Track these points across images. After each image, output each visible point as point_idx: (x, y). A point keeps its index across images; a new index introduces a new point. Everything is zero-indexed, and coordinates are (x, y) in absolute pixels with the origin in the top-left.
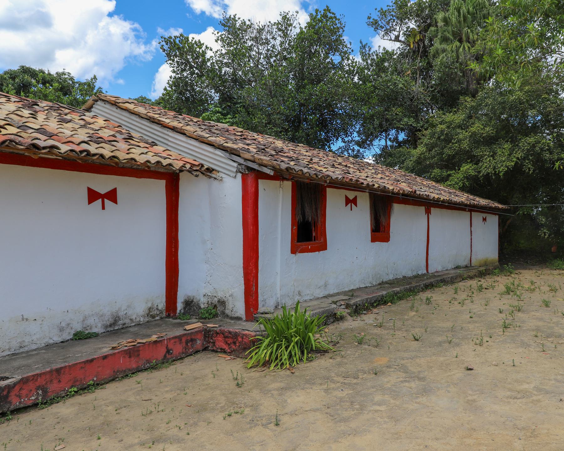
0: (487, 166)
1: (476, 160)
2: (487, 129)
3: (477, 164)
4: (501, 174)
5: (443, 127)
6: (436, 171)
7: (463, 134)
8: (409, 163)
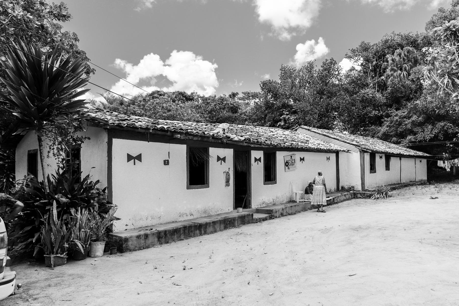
0: (420, 137)
1: (415, 134)
2: (420, 119)
3: (415, 135)
4: (428, 140)
5: (397, 118)
6: (394, 139)
8: (380, 135)
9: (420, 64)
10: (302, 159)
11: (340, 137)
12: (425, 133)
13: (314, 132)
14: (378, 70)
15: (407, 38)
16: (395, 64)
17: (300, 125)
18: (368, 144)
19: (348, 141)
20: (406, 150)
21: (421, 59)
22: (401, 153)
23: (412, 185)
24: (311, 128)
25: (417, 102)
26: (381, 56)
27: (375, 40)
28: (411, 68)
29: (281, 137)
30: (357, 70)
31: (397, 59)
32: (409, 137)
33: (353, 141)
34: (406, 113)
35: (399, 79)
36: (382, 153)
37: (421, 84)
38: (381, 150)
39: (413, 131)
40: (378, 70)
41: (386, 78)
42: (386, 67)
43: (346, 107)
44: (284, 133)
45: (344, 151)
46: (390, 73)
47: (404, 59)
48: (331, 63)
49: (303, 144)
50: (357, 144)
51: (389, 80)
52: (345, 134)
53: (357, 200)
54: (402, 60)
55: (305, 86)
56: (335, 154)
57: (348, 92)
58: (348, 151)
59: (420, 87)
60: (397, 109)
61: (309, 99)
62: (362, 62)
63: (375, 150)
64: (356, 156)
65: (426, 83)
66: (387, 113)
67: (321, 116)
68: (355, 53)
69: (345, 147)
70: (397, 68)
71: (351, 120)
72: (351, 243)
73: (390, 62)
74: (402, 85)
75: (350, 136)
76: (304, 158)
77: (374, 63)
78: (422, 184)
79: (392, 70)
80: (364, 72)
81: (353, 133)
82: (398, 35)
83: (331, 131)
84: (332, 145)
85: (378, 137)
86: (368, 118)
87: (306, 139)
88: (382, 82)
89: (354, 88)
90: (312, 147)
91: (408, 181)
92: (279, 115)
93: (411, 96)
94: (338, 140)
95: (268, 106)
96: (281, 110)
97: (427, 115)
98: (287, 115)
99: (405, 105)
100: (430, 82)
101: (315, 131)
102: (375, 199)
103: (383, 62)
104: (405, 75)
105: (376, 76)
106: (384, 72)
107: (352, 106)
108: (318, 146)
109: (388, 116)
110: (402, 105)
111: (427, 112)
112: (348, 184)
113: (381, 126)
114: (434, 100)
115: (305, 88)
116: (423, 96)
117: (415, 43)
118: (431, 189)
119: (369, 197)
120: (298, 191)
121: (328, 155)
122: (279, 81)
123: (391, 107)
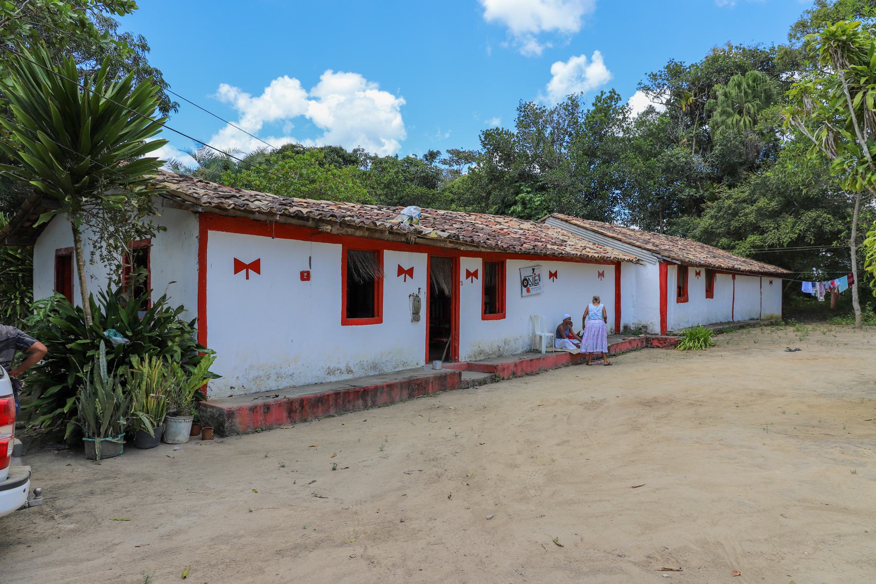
0: (771, 238)
1: (762, 232)
4: (785, 245)
5: (730, 202)
6: (724, 241)
7: (749, 209)
8: (697, 232)
9: (776, 103)
10: (553, 275)
11: (624, 234)
12: (782, 231)
13: (575, 225)
14: (697, 113)
15: (753, 54)
16: (730, 101)
17: (551, 212)
18: (675, 249)
19: (638, 244)
20: (744, 262)
21: (779, 94)
22: (736, 266)
23: (754, 326)
24: (570, 218)
25: (768, 174)
26: (704, 87)
27: (693, 56)
28: (758, 111)
29: (516, 233)
30: (658, 113)
31: (734, 92)
32: (751, 238)
33: (647, 242)
34: (747, 194)
35: (736, 130)
36: (700, 265)
37: (777, 140)
38: (698, 260)
39: (759, 227)
40: (698, 113)
41: (713, 127)
42: (713, 107)
43: (636, 181)
44: (522, 226)
45: (629, 261)
46: (719, 120)
47: (746, 93)
48: (611, 98)
49: (555, 247)
50: (654, 248)
51: (718, 132)
52: (633, 230)
53: (652, 350)
54: (743, 94)
55: (563, 140)
56: (613, 267)
57: (640, 153)
58: (638, 262)
59: (775, 147)
60: (730, 187)
61: (569, 164)
62: (668, 97)
63: (687, 260)
64: (652, 271)
65: (786, 139)
66: (713, 194)
67: (591, 196)
68: (656, 79)
69: (632, 253)
70: (733, 109)
71: (644, 204)
72: (639, 429)
73: (721, 98)
74: (742, 142)
75: (641, 235)
76: (556, 272)
77: (691, 99)
78: (772, 324)
79: (724, 112)
80: (672, 117)
81: (648, 228)
82: (737, 47)
83: (607, 224)
84: (609, 249)
85: (694, 237)
86: (677, 201)
87: (561, 238)
88: (704, 136)
89: (652, 145)
90: (573, 252)
91: (747, 318)
92: (512, 194)
93: (758, 162)
94: (620, 240)
95: (494, 176)
96: (517, 184)
97: (785, 197)
98: (528, 192)
99: (746, 179)
100: (793, 137)
101: (578, 223)
102: (685, 349)
103: (708, 98)
104: (747, 122)
105: (693, 124)
106: (709, 117)
107: (649, 178)
108: (584, 252)
109: (714, 198)
110: (740, 178)
111: (785, 191)
112: (636, 321)
113: (699, 216)
114: (800, 169)
115: (561, 145)
116: (780, 163)
117: (768, 63)
118: (790, 332)
119: (675, 345)
120: (546, 333)
121: (601, 268)
122: (515, 131)
123: (719, 182)
